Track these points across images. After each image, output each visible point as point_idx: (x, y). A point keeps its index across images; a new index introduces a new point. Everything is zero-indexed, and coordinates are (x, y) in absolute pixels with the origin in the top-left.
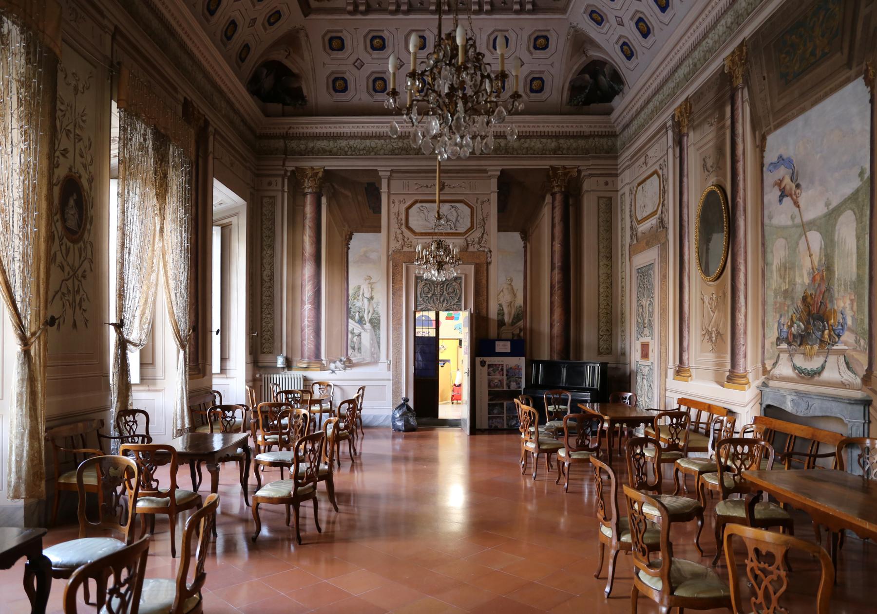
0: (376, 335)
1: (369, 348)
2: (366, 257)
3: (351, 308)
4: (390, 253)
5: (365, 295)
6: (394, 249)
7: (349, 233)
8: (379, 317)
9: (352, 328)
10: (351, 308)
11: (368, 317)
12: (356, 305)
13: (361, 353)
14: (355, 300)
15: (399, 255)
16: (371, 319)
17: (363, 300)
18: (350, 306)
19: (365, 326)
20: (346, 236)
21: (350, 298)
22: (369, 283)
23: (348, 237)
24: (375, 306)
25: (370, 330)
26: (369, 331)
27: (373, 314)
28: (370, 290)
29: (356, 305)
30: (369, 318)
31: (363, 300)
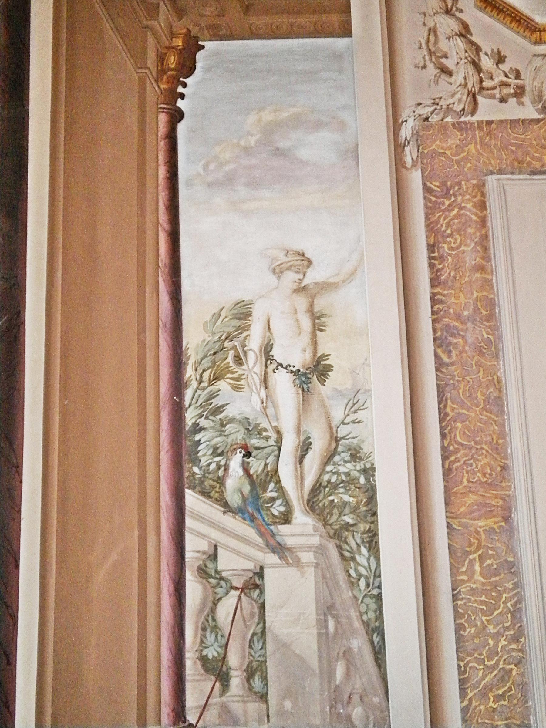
0: (353, 584)
1: (314, 663)
2: (279, 152)
3: (197, 429)
4: (406, 132)
5: (276, 352)
6: (425, 111)
7: (179, 42)
8: (369, 472)
9: (204, 546)
10: (197, 429)
11: (301, 478)
12: (230, 412)
13: (264, 697)
14: (223, 385)
15: (454, 139)
16: (317, 488)
17: (265, 382)
18: (190, 417)
19: (283, 529)
20: (161, 59)
21: (189, 372)
22: (301, 289)
23: (172, 61)
24: (337, 414)
25: (320, 550)
26: (307, 557)
27: (329, 459)
28: (306, 323)
29: (230, 412)
30: (309, 482)
31: (265, 382)
